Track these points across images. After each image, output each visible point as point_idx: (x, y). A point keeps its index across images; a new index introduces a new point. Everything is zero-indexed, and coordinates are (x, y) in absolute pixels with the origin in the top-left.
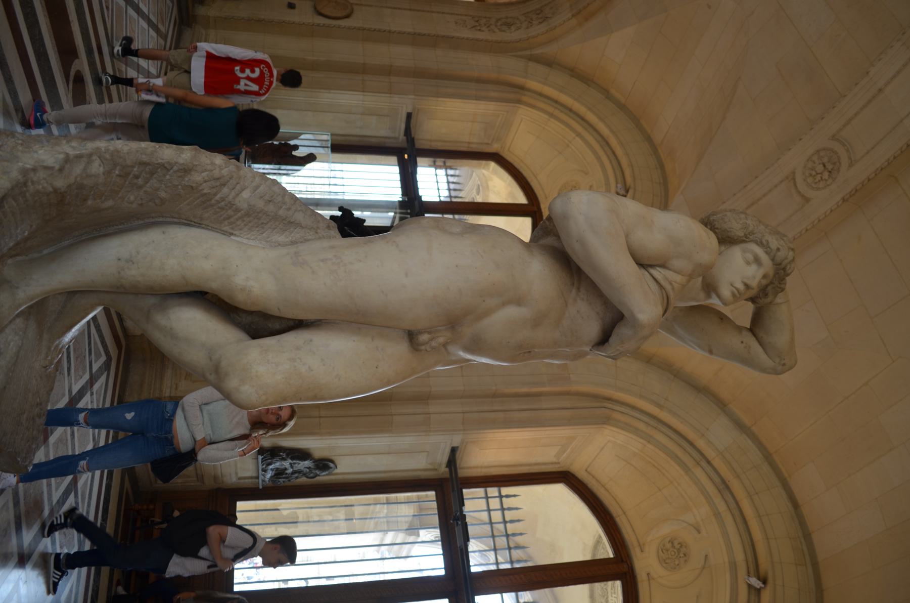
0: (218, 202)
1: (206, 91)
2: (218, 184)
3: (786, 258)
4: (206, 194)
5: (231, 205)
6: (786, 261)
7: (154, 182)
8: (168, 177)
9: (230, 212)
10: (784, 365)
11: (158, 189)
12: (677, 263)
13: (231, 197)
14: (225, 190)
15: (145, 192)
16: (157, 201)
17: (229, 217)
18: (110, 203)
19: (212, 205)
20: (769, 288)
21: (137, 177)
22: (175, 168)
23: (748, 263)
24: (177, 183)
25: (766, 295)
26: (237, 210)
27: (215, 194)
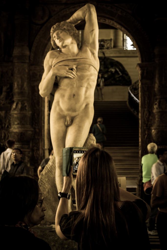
0: (50, 169)
1: (126, 179)
2: (46, 169)
3: (52, 30)
4: (48, 172)
5: (51, 166)
6: (53, 30)
7: (44, 181)
8: (43, 178)
9: (53, 167)
10: (86, 10)
11: (45, 181)
12: (50, 64)
13: (49, 166)
14: (48, 168)
15: (46, 183)
16: (48, 181)
17: (54, 167)
18: (47, 190)
19: (51, 170)
20: (62, 29)
21: (42, 184)
22: (42, 177)
23: (56, 39)
24: (44, 177)
25: (65, 29)
26: (52, 165)
27: (48, 169)
